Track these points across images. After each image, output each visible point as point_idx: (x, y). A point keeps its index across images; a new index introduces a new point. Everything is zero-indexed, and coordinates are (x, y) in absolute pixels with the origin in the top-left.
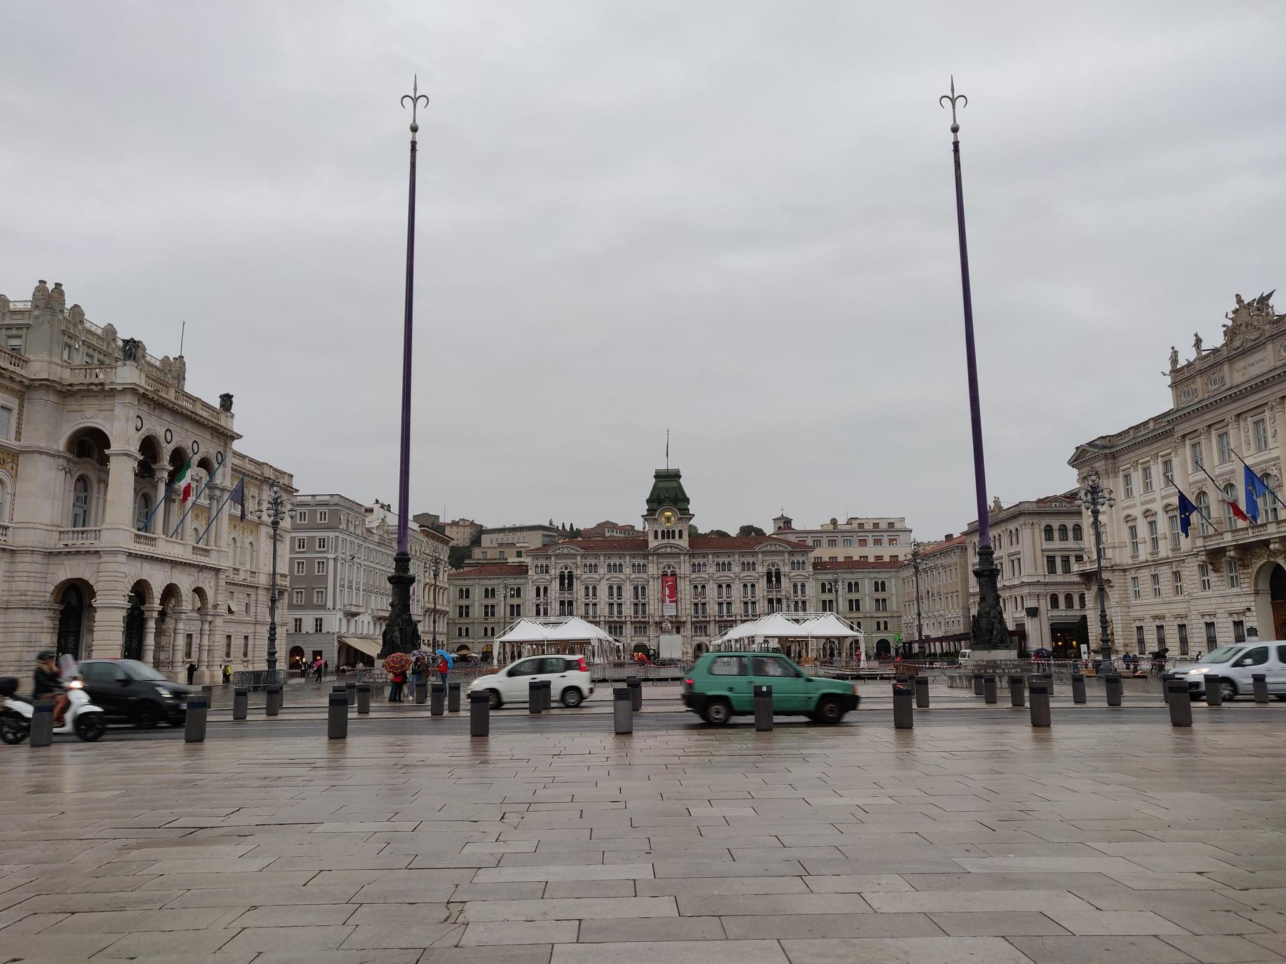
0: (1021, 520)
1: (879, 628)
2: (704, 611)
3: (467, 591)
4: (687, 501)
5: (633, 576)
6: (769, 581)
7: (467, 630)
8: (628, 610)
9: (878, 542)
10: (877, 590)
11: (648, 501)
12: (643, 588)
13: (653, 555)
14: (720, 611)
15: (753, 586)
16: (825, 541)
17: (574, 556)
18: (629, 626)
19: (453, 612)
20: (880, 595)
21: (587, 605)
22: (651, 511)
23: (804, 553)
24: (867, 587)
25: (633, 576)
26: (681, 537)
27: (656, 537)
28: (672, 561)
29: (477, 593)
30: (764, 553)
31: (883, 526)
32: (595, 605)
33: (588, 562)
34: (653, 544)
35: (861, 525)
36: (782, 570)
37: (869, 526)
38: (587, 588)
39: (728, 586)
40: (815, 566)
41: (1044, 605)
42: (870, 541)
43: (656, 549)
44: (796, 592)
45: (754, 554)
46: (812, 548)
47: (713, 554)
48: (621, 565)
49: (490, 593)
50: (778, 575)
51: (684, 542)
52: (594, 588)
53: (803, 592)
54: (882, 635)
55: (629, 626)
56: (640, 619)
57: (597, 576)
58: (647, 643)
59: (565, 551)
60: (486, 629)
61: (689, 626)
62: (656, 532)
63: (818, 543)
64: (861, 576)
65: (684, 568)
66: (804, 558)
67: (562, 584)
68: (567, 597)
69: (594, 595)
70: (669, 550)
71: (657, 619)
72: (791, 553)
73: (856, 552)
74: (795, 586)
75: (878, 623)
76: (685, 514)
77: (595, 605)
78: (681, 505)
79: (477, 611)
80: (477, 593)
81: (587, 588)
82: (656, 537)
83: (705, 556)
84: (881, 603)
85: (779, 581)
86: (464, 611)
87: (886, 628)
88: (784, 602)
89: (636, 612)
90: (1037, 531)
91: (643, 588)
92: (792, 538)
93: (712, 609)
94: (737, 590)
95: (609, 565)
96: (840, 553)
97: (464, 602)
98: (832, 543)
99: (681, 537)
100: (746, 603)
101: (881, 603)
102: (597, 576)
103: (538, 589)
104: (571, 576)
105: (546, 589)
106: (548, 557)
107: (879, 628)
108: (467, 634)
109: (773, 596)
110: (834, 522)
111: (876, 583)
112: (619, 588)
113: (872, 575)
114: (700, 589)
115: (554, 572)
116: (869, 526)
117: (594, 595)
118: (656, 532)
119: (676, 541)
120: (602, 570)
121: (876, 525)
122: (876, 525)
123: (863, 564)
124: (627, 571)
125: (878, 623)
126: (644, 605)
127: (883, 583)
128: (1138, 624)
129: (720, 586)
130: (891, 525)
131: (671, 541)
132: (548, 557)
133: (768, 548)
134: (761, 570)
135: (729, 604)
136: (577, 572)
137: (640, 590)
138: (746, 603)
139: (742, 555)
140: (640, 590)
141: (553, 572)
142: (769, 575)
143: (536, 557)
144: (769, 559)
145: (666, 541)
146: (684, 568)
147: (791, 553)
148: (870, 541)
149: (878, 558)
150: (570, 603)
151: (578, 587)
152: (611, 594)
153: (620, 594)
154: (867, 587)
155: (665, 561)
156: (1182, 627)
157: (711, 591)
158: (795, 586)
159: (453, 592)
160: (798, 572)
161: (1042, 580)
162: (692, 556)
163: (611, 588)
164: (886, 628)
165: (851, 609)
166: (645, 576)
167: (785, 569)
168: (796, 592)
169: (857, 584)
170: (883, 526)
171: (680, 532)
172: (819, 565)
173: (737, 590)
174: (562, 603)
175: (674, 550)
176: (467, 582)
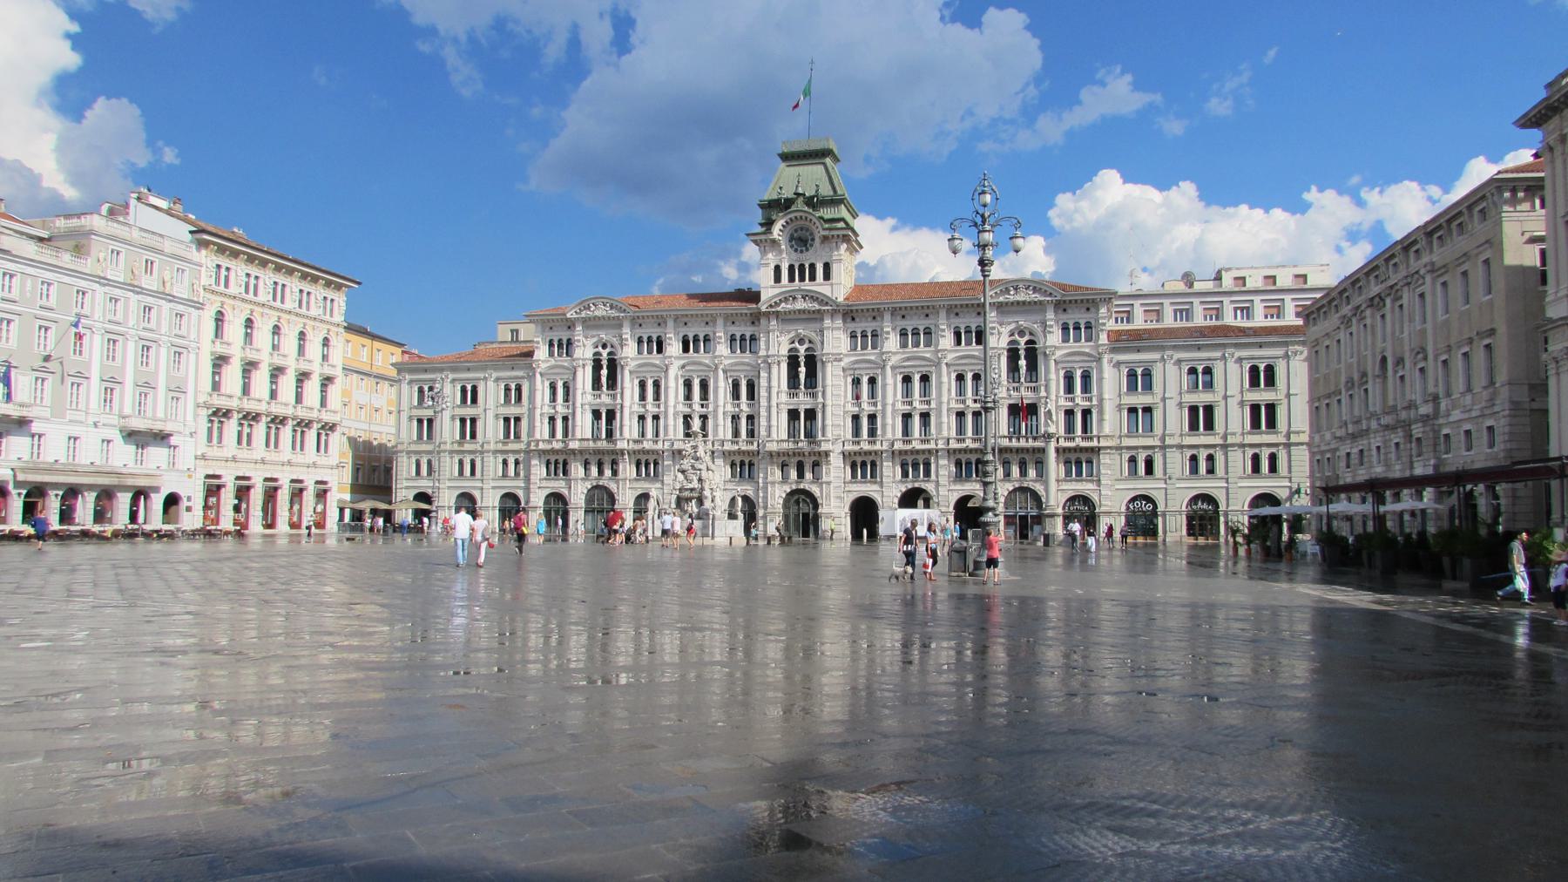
6: (1013, 368)
20: (1263, 396)
21: (642, 418)
26: (827, 276)
27: (778, 279)
32: (656, 417)
38: (642, 385)
39: (925, 379)
44: (1069, 388)
48: (707, 339)
49: (471, 395)
61: (836, 461)
62: (777, 269)
65: (835, 340)
70: (800, 305)
81: (642, 385)
82: (778, 279)
93: (891, 429)
99: (827, 276)
100: (960, 415)
104: (613, 365)
112: (704, 386)
114: (865, 383)
118: (777, 269)
119: (819, 286)
120: (674, 348)
124: (722, 349)
131: (807, 285)
132: (570, 325)
142: (1013, 354)
150: (611, 415)
163: (688, 385)
164: (1273, 468)
165: (1194, 426)
168: (1069, 388)
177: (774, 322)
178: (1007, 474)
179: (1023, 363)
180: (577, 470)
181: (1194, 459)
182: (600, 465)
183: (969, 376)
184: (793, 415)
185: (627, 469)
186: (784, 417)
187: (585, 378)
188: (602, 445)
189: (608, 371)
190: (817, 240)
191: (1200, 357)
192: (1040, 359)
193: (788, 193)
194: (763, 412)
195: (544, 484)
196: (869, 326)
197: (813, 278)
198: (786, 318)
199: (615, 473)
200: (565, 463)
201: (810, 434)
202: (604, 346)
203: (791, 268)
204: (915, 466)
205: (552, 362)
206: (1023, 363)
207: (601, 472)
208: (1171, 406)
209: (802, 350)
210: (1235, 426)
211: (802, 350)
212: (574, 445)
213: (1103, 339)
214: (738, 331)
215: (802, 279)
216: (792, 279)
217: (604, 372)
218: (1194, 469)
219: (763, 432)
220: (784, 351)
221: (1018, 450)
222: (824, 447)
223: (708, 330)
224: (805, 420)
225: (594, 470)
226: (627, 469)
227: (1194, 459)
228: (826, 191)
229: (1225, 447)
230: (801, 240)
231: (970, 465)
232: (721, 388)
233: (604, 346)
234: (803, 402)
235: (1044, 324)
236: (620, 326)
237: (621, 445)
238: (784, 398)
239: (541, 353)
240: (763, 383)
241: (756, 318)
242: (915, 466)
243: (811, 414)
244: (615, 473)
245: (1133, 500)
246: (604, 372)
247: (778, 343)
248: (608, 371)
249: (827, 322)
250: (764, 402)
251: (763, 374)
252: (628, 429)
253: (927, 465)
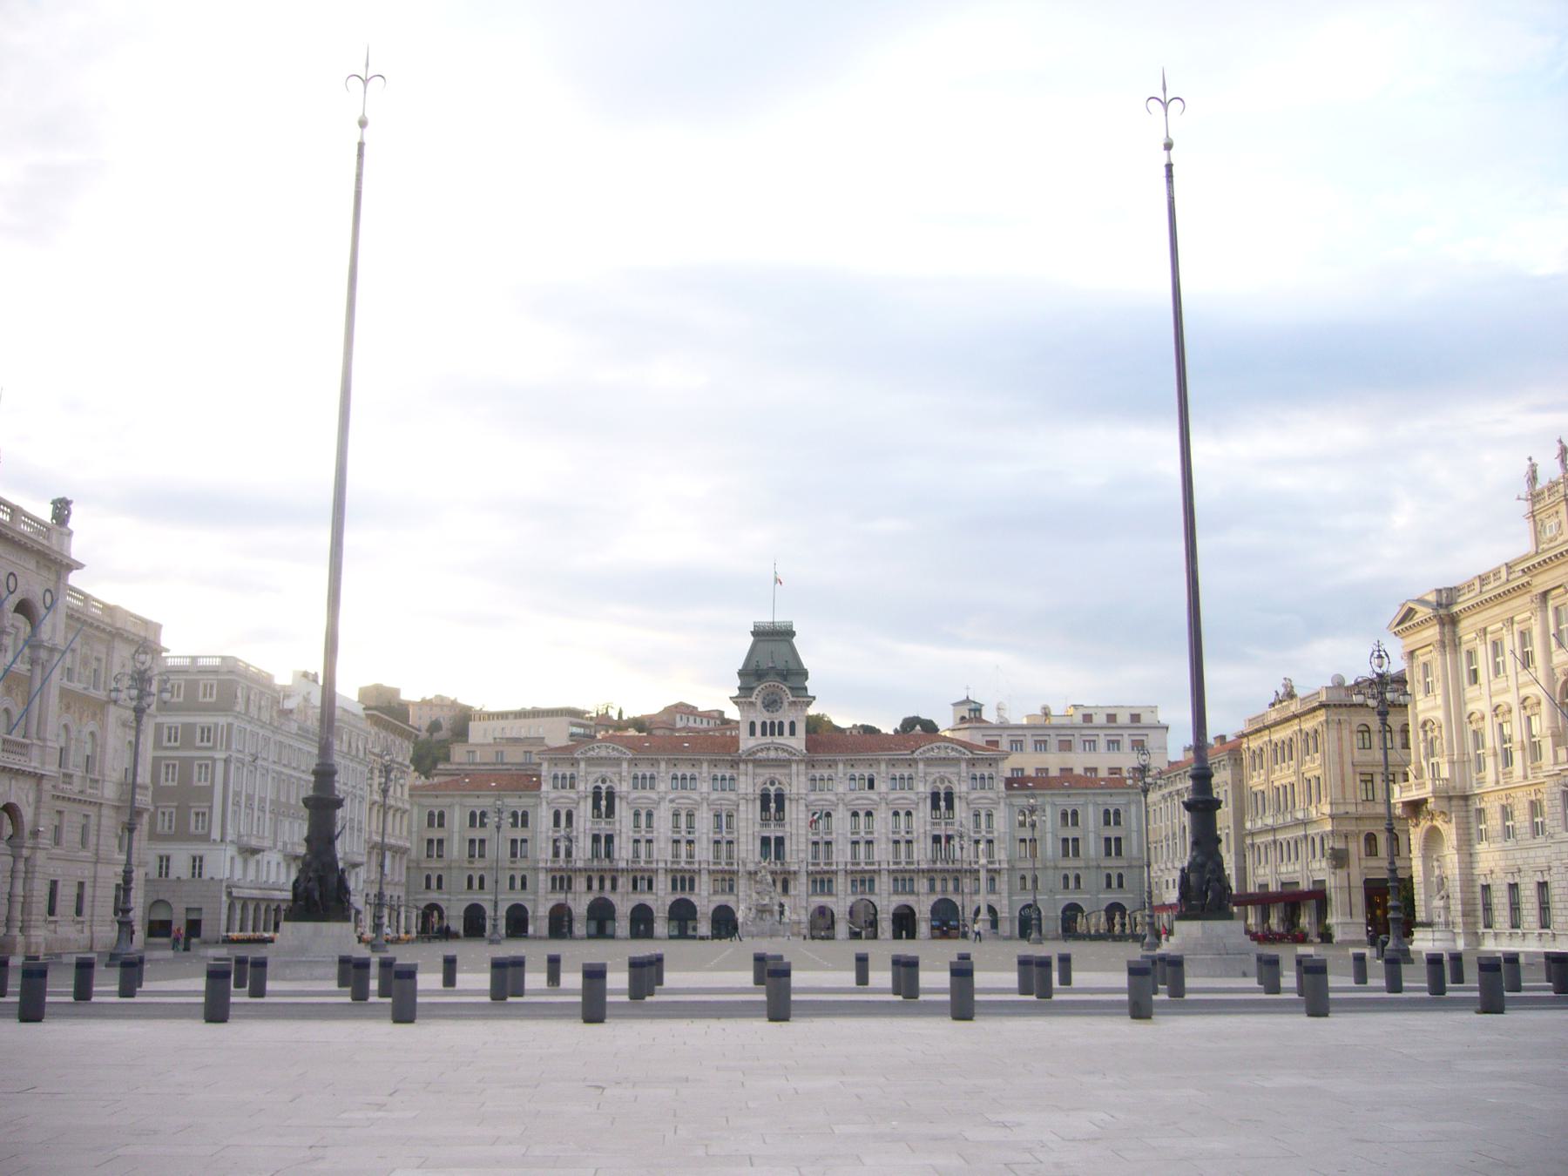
0: (1321, 716)
1: (1109, 885)
2: (829, 854)
3: (441, 815)
4: (804, 674)
5: (714, 796)
7: (440, 878)
8: (704, 852)
9: (1114, 744)
10: (1107, 823)
11: (741, 674)
12: (730, 816)
13: (746, 762)
14: (854, 855)
15: (909, 814)
16: (1029, 743)
17: (617, 762)
18: (705, 878)
19: (417, 849)
21: (637, 841)
22: (745, 690)
23: (992, 762)
24: (1091, 817)
25: (714, 796)
26: (792, 733)
27: (752, 733)
28: (777, 773)
29: (457, 819)
30: (929, 762)
31: (1123, 719)
32: (649, 841)
33: (640, 771)
34: (747, 743)
35: (1088, 718)
36: (956, 789)
37: (1100, 719)
38: (637, 814)
40: (1009, 783)
41: (1356, 848)
42: (1102, 743)
43: (751, 752)
44: (977, 825)
45: (912, 763)
46: (1005, 756)
47: (845, 762)
48: (693, 778)
50: (949, 797)
51: (798, 742)
52: (650, 815)
53: (989, 826)
54: (1113, 896)
55: (705, 878)
56: (724, 866)
57: (653, 795)
58: (732, 905)
59: (603, 753)
60: (470, 879)
61: (803, 878)
62: (752, 725)
63: (1017, 745)
64: (1082, 800)
66: (992, 770)
67: (596, 806)
68: (603, 827)
69: (649, 825)
70: (772, 754)
71: (751, 867)
72: (972, 763)
73: (1078, 761)
74: (977, 815)
75: (1109, 877)
76: (802, 696)
77: (649, 841)
78: (794, 682)
79: (456, 849)
80: (457, 819)
82: (752, 733)
83: (832, 764)
84: (1113, 846)
85: (950, 806)
86: (435, 847)
87: (1120, 885)
88: (956, 842)
89: (717, 857)
90: (1346, 733)
91: (730, 816)
92: (978, 738)
93: (842, 855)
94: (882, 825)
95: (675, 778)
96: (1053, 762)
97: (436, 834)
98: (1041, 745)
99: (792, 733)
101: (1113, 846)
102: (653, 795)
103: (557, 815)
104: (611, 796)
105: (569, 815)
106: (575, 763)
107: (1109, 885)
108: (439, 887)
109: (941, 831)
110: (1046, 713)
111: (1107, 812)
112: (690, 815)
113: (1100, 800)
115: (584, 787)
116: (1100, 719)
117: (649, 825)
118: (752, 725)
119: (786, 740)
120: (662, 787)
121: (1112, 718)
122: (1112, 718)
123: (1086, 782)
124: (705, 787)
125: (1109, 877)
126: (730, 842)
127: (1117, 813)
128: (1482, 881)
129: (855, 814)
130: (1135, 718)
131: (778, 739)
132: (575, 763)
133: (934, 754)
134: (924, 789)
135: (869, 843)
136: (623, 788)
137: (725, 819)
138: (896, 842)
139: (892, 763)
140: (725, 819)
141: (581, 787)
142: (935, 797)
143: (554, 762)
144: (936, 771)
145: (768, 739)
146: (796, 784)
147: (972, 763)
148: (1102, 743)
149: (1114, 771)
150: (610, 839)
151: (623, 812)
152: (676, 826)
153: (690, 827)
154: (1091, 817)
155: (767, 773)
156: (1543, 886)
157: (841, 823)
158: (977, 815)
159: (418, 817)
160: (981, 793)
161: (1351, 809)
162: (812, 764)
163: (676, 815)
164: (1120, 885)
165: (1066, 854)
166: (732, 796)
167: (961, 788)
168: (977, 825)
169: (1075, 813)
170: (1123, 719)
171: (792, 724)
172: (1016, 782)
173: (882, 825)
174: (596, 838)
175: (785, 755)
176: (439, 801)
177: (750, 766)
178: (932, 889)
179: (943, 804)
180: (580, 884)
181: (1066, 878)
182: (602, 880)
183: (902, 814)
184: (765, 841)
185: (624, 883)
186: (758, 843)
187: (585, 810)
188: (606, 864)
189: (604, 802)
190: (786, 704)
191: (1068, 803)
192: (956, 801)
193: (763, 666)
194: (742, 839)
195: (550, 896)
196: (826, 773)
197: (781, 733)
198: (759, 763)
199: (614, 887)
200: (570, 879)
201: (779, 855)
202: (604, 781)
203: (764, 724)
204: (863, 882)
205: (553, 794)
206: (943, 804)
207: (602, 887)
208: (1049, 836)
209: (772, 790)
210: (1092, 852)
211: (772, 790)
212: (580, 864)
213: (1002, 786)
214: (719, 772)
215: (772, 734)
216: (764, 734)
217: (603, 803)
218: (1066, 886)
219: (743, 855)
220: (758, 792)
221: (942, 871)
222: (794, 868)
223: (695, 771)
224: (773, 847)
225: (596, 884)
226: (624, 883)
227: (1066, 878)
228: (792, 666)
229: (1087, 868)
230: (772, 704)
231: (903, 879)
232: (704, 824)
233: (604, 781)
234: (772, 832)
235: (959, 774)
236: (619, 765)
237: (622, 865)
238: (757, 828)
239: (545, 787)
240: (742, 815)
241: (735, 764)
242: (863, 882)
243: (780, 841)
244: (614, 887)
245: (1023, 908)
246: (603, 803)
247: (748, 784)
248: (604, 802)
249: (794, 767)
250: (742, 831)
251: (742, 808)
252: (623, 852)
253: (872, 881)
